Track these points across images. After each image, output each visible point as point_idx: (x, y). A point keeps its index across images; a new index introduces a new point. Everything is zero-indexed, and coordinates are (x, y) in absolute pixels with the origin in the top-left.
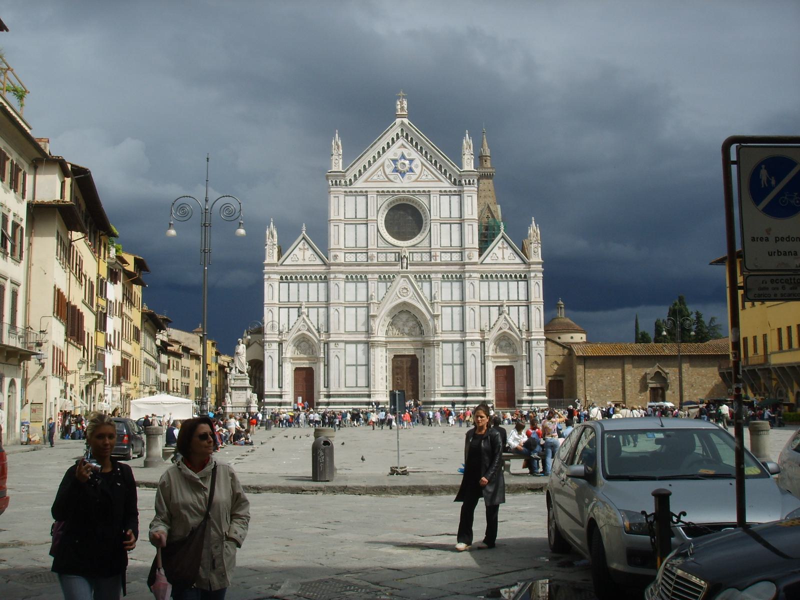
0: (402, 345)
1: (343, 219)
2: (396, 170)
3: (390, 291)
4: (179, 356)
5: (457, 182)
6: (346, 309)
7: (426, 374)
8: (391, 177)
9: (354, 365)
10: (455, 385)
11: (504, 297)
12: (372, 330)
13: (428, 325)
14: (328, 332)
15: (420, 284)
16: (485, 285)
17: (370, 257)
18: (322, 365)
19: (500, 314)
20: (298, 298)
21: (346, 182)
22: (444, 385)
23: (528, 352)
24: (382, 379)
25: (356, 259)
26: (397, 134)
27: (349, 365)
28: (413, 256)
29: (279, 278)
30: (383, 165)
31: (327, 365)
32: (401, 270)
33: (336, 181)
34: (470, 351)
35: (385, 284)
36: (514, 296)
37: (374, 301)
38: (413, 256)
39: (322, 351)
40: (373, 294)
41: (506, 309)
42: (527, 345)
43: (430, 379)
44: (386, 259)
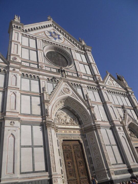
0: (68, 132)
9: (30, 147)
10: (119, 162)
12: (47, 113)
27: (24, 147)
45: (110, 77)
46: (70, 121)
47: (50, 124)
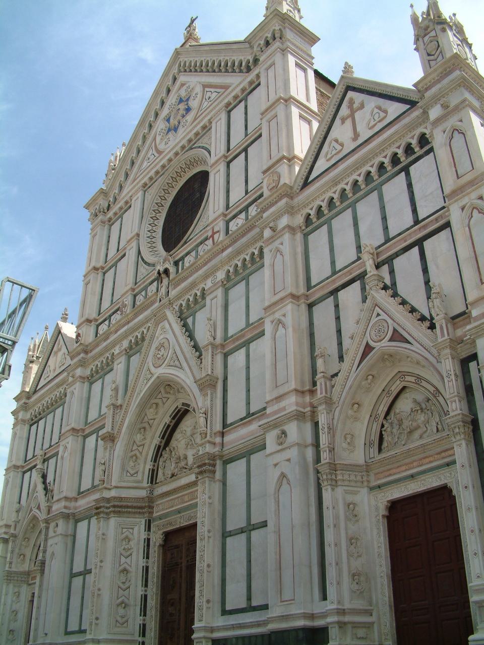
8: (161, 147)
9: (80, 574)
22: (228, 607)
30: (155, 139)
34: (276, 465)
47: (100, 507)
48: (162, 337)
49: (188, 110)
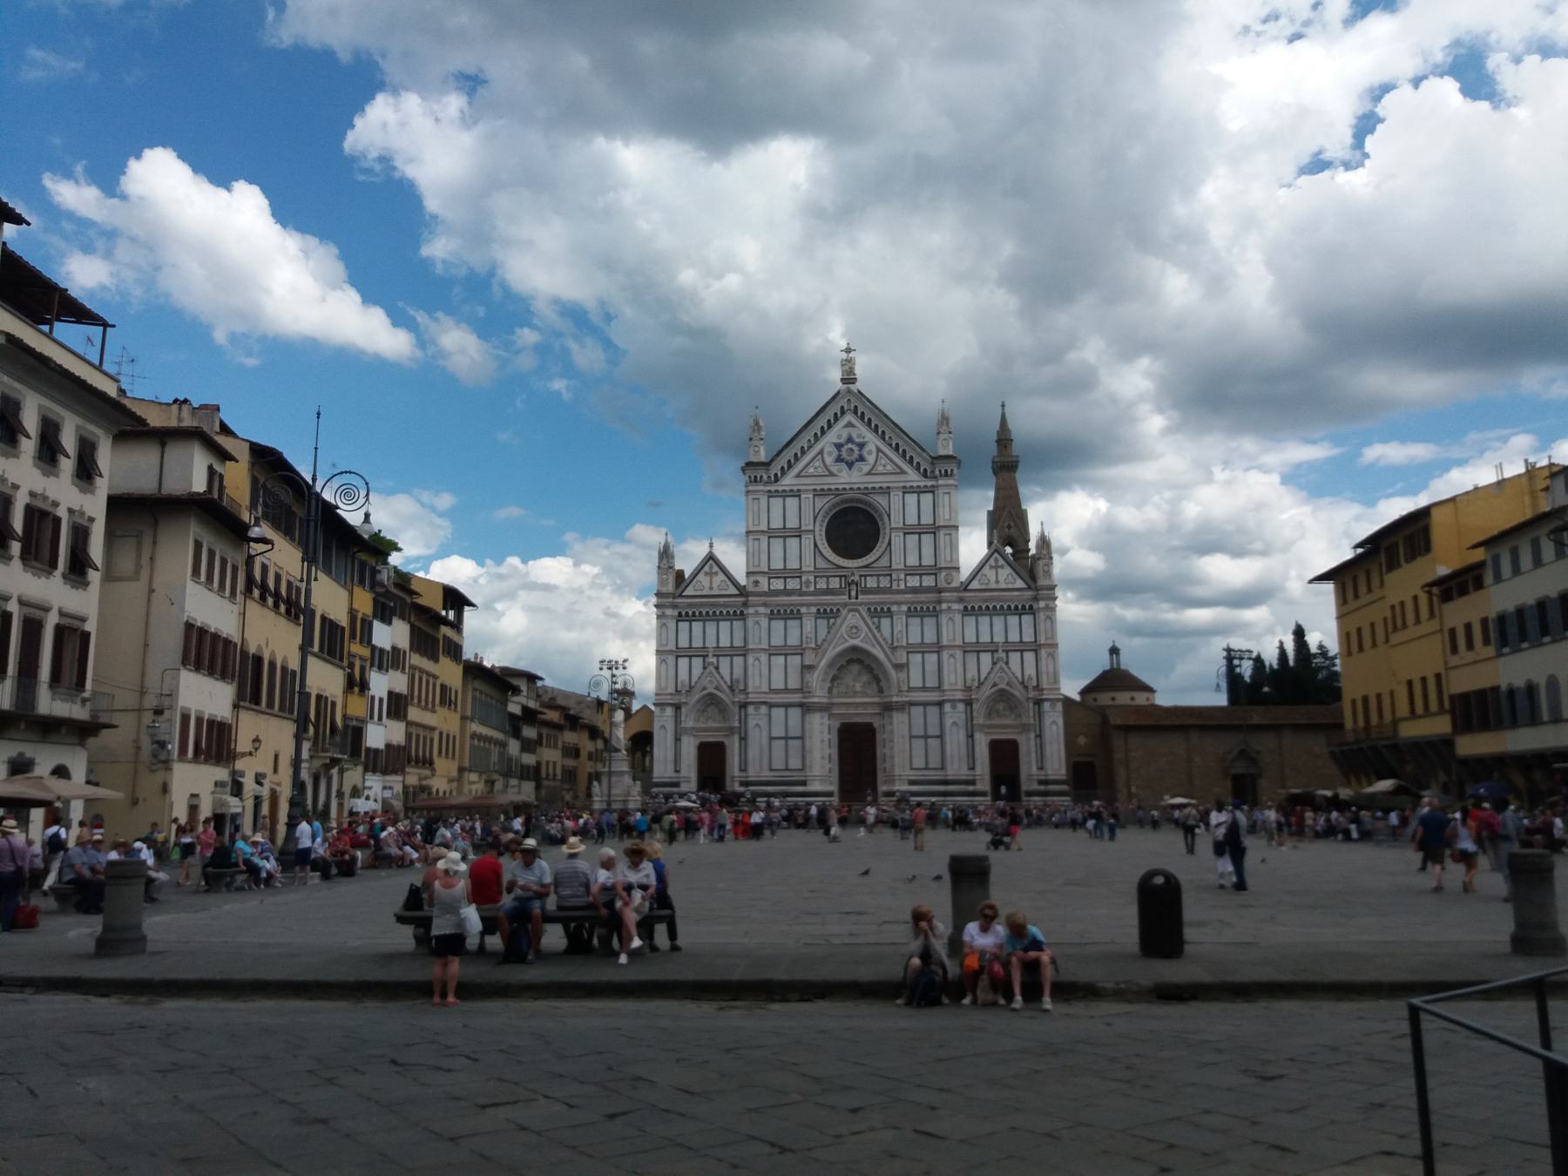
1: (766, 529)
2: (839, 459)
3: (833, 631)
4: (558, 727)
5: (929, 474)
6: (772, 657)
7: (887, 751)
8: (834, 469)
10: (931, 766)
11: (999, 638)
13: (888, 680)
14: (745, 690)
15: (876, 620)
16: (970, 621)
17: (805, 583)
18: (736, 738)
19: (994, 663)
20: (704, 642)
21: (769, 477)
23: (1037, 719)
24: (823, 758)
25: (785, 587)
26: (842, 407)
28: (865, 580)
29: (676, 613)
30: (821, 452)
31: (744, 739)
32: (848, 600)
33: (756, 477)
35: (825, 621)
36: (1014, 637)
37: (810, 645)
38: (865, 580)
39: (737, 718)
40: (809, 635)
41: (1004, 655)
42: (1037, 710)
43: (892, 758)
44: (828, 585)
45: (996, 555)
46: (862, 687)
48: (853, 621)
49: (861, 459)
